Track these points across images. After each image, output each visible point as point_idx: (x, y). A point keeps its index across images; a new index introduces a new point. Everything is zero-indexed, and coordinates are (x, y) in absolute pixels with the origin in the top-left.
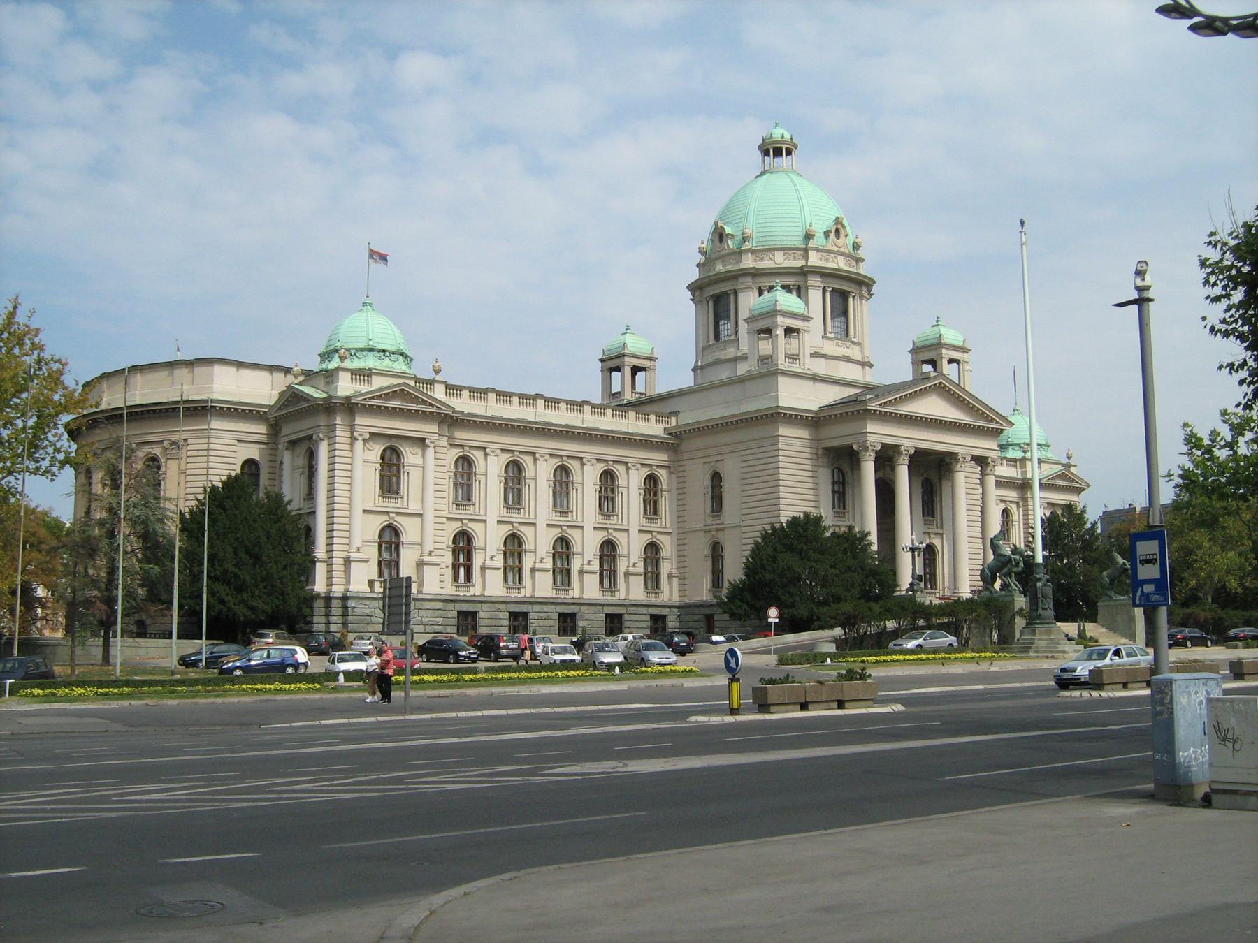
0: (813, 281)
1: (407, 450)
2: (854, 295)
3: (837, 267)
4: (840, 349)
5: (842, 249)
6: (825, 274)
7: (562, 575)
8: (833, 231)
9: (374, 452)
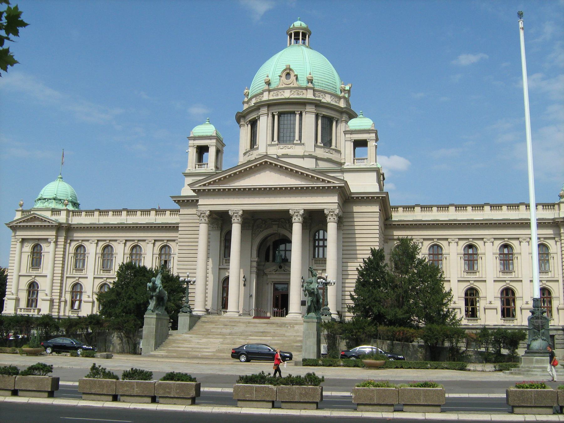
0: (264, 110)
1: (44, 244)
2: (300, 112)
3: (283, 97)
4: (282, 150)
5: (291, 85)
6: (270, 105)
8: (284, 75)
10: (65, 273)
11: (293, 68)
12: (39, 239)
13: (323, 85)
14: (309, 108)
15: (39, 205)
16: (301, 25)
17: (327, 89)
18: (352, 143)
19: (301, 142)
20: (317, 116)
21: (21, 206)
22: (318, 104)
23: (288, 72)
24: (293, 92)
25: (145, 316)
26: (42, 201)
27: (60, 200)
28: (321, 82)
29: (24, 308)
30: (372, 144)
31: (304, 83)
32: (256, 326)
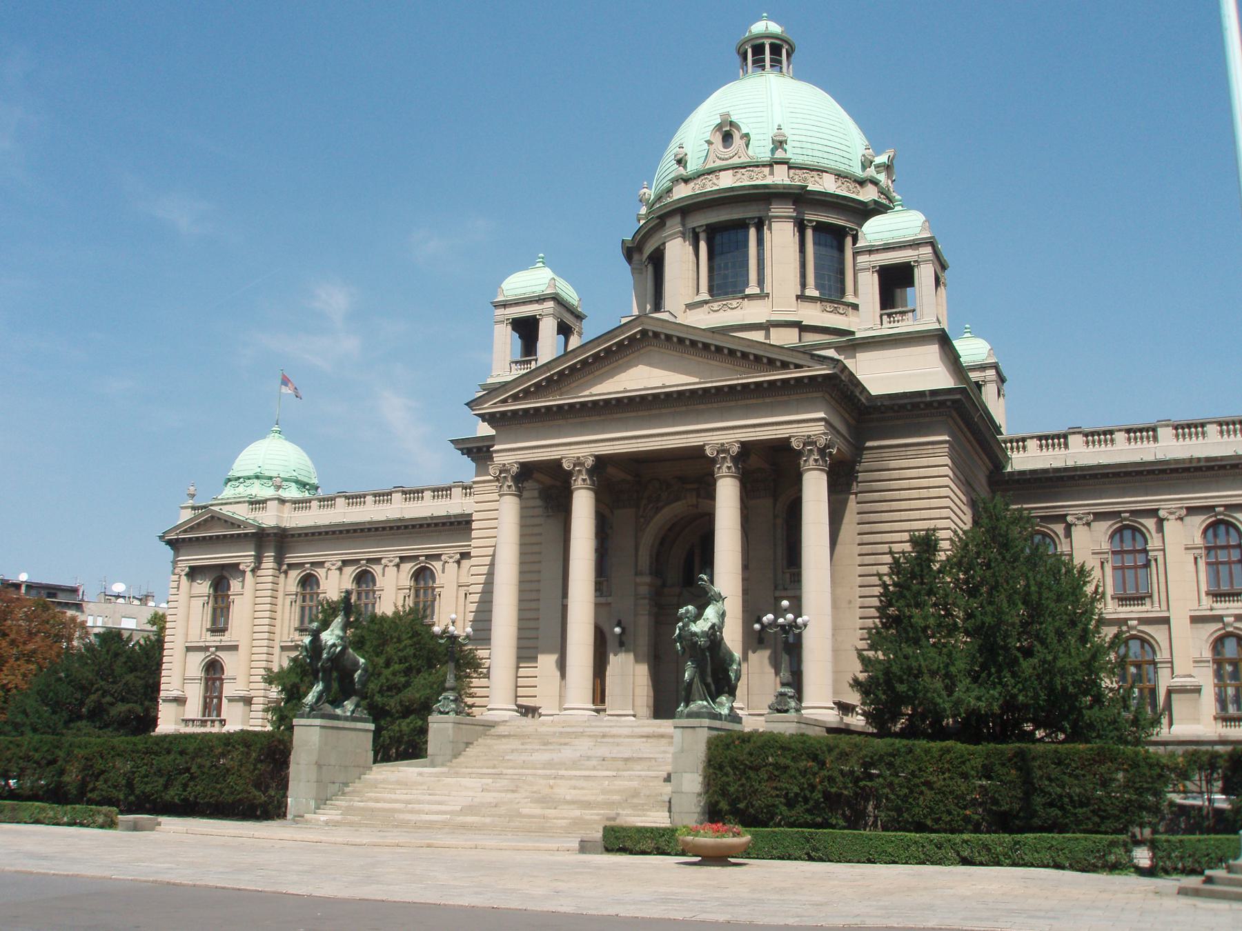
0: (674, 225)
2: (756, 220)
5: (736, 161)
6: (686, 210)
8: (718, 139)
10: (277, 637)
11: (743, 120)
12: (223, 566)
13: (816, 153)
14: (776, 210)
15: (229, 492)
16: (767, 27)
17: (826, 161)
18: (876, 275)
19: (762, 289)
20: (801, 226)
21: (193, 496)
22: (800, 198)
23: (727, 131)
24: (739, 175)
25: (295, 721)
26: (233, 483)
27: (271, 478)
28: (809, 146)
30: (924, 275)
31: (764, 154)
32: (618, 745)
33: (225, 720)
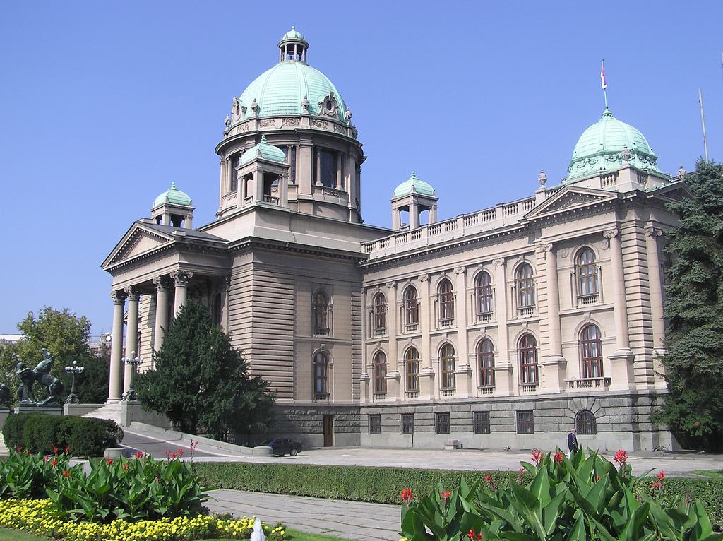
7: (487, 377)
9: (569, 258)
29: (578, 379)
33: (609, 380)
